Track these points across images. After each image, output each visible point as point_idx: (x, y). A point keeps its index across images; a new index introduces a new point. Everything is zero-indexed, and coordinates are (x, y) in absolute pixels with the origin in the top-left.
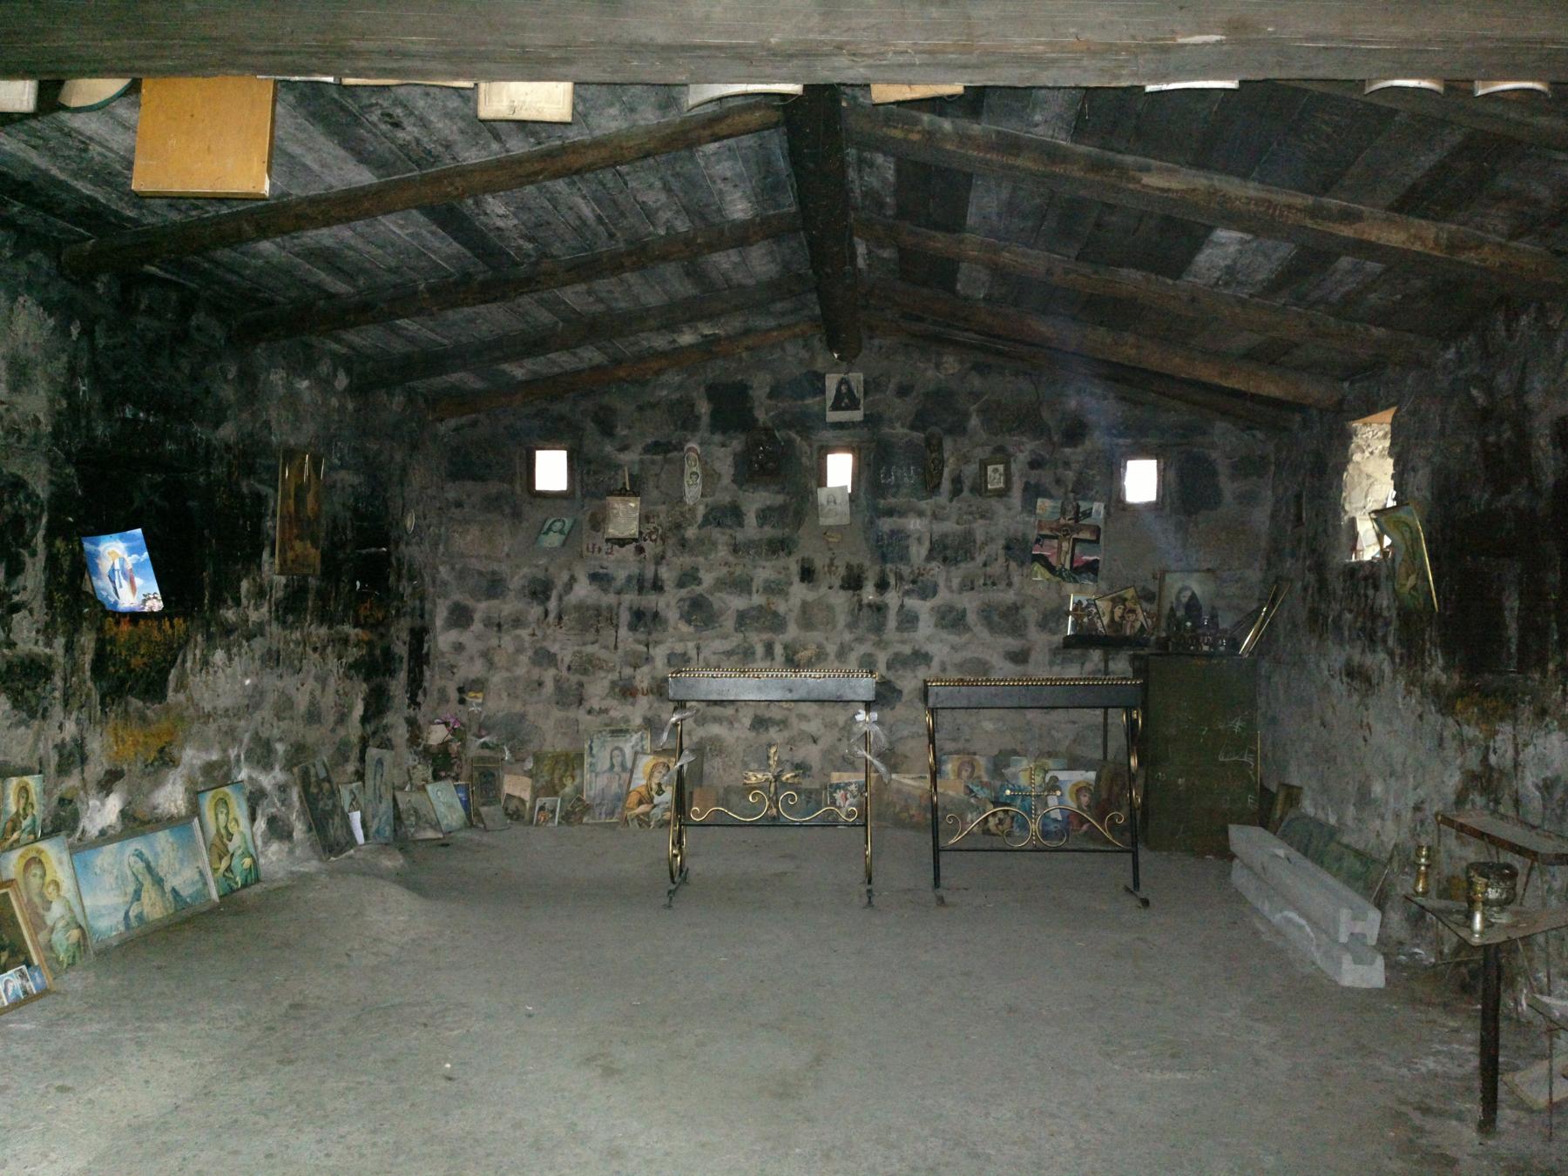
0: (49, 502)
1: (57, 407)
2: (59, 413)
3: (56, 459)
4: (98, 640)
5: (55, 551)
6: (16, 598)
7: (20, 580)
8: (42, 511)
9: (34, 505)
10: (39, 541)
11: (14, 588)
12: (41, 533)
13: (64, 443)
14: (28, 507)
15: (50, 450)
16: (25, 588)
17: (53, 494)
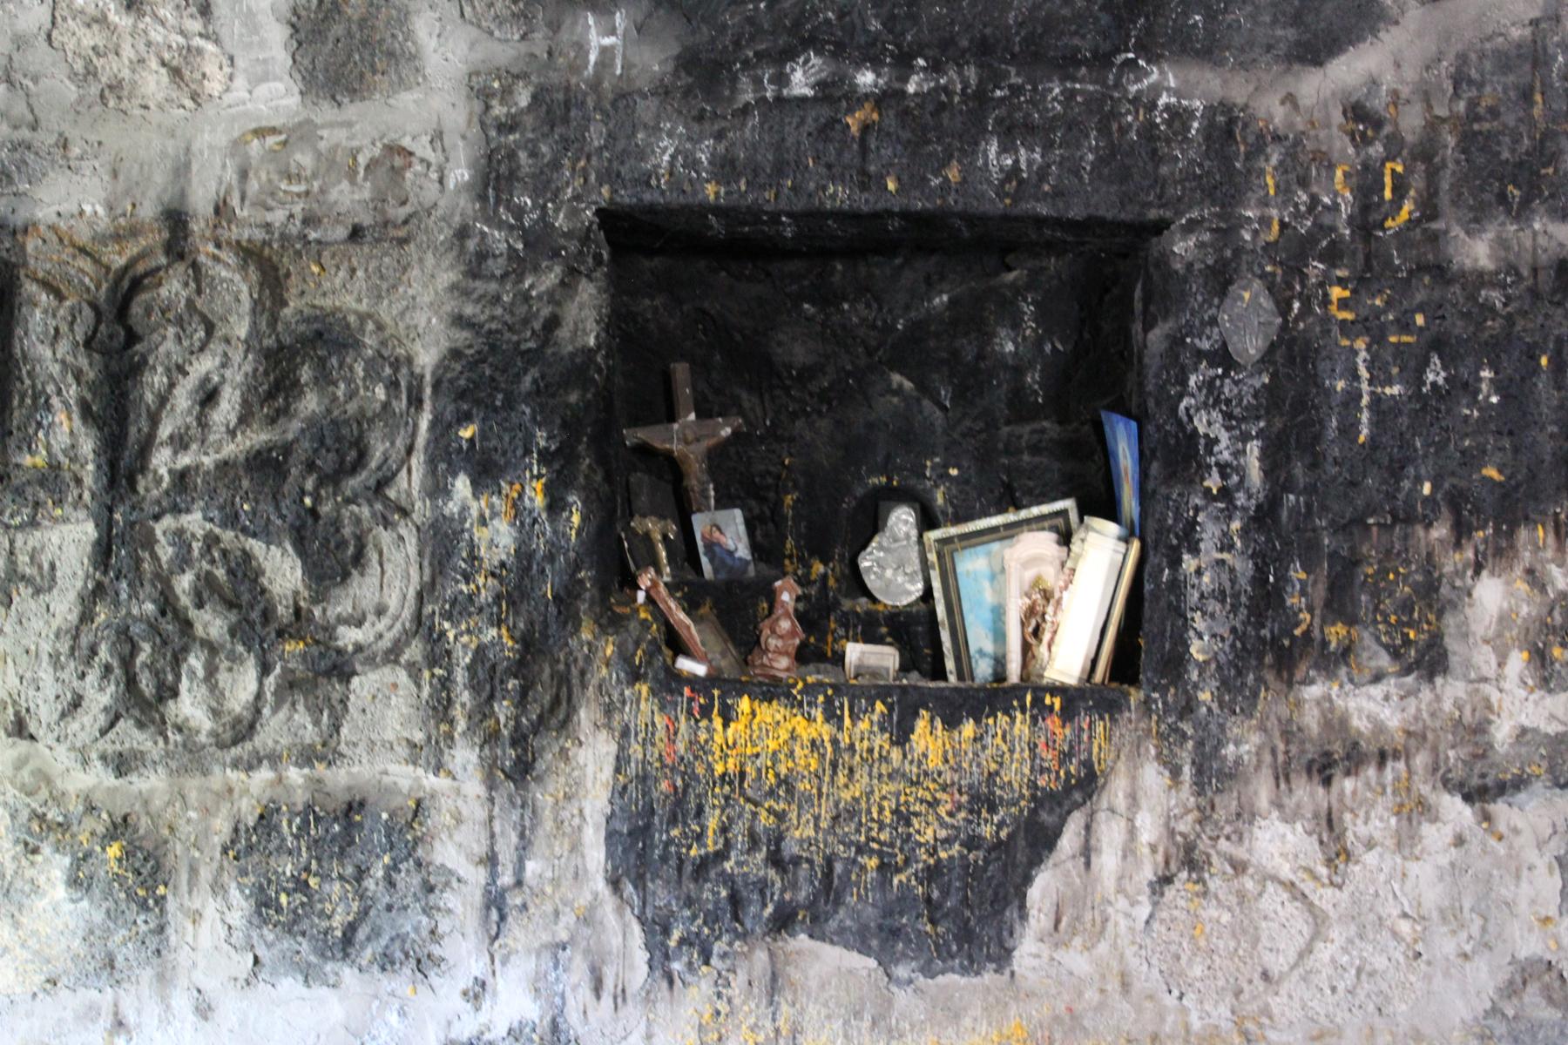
0: (433, 374)
1: (498, 110)
2: (506, 127)
3: (482, 256)
4: (621, 762)
5: (452, 508)
6: (349, 636)
7: (362, 590)
8: (416, 401)
9: (393, 385)
10: (411, 482)
11: (341, 606)
12: (417, 461)
13: (519, 212)
14: (380, 392)
15: (463, 233)
16: (380, 611)
17: (455, 354)
